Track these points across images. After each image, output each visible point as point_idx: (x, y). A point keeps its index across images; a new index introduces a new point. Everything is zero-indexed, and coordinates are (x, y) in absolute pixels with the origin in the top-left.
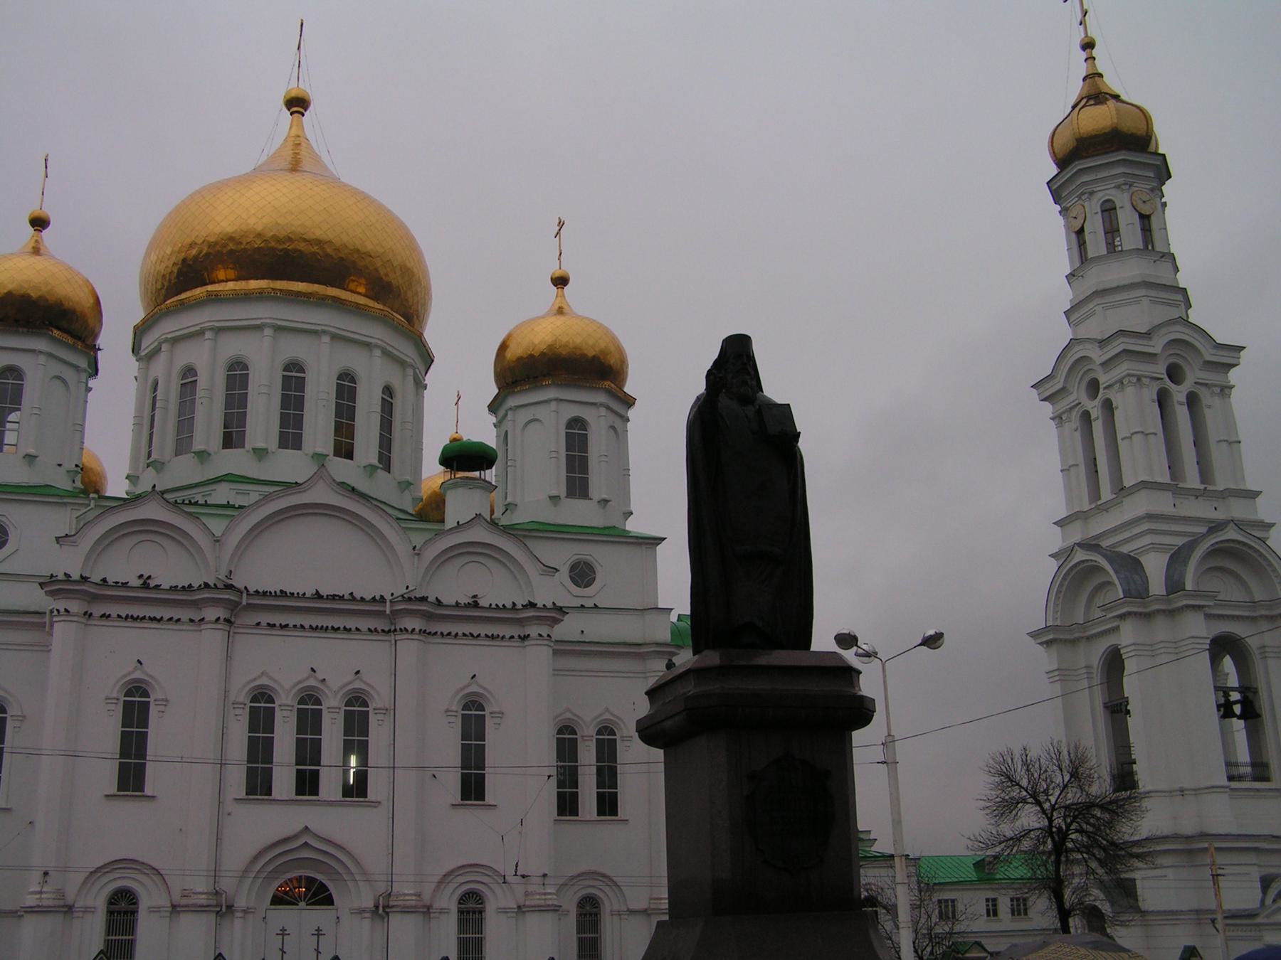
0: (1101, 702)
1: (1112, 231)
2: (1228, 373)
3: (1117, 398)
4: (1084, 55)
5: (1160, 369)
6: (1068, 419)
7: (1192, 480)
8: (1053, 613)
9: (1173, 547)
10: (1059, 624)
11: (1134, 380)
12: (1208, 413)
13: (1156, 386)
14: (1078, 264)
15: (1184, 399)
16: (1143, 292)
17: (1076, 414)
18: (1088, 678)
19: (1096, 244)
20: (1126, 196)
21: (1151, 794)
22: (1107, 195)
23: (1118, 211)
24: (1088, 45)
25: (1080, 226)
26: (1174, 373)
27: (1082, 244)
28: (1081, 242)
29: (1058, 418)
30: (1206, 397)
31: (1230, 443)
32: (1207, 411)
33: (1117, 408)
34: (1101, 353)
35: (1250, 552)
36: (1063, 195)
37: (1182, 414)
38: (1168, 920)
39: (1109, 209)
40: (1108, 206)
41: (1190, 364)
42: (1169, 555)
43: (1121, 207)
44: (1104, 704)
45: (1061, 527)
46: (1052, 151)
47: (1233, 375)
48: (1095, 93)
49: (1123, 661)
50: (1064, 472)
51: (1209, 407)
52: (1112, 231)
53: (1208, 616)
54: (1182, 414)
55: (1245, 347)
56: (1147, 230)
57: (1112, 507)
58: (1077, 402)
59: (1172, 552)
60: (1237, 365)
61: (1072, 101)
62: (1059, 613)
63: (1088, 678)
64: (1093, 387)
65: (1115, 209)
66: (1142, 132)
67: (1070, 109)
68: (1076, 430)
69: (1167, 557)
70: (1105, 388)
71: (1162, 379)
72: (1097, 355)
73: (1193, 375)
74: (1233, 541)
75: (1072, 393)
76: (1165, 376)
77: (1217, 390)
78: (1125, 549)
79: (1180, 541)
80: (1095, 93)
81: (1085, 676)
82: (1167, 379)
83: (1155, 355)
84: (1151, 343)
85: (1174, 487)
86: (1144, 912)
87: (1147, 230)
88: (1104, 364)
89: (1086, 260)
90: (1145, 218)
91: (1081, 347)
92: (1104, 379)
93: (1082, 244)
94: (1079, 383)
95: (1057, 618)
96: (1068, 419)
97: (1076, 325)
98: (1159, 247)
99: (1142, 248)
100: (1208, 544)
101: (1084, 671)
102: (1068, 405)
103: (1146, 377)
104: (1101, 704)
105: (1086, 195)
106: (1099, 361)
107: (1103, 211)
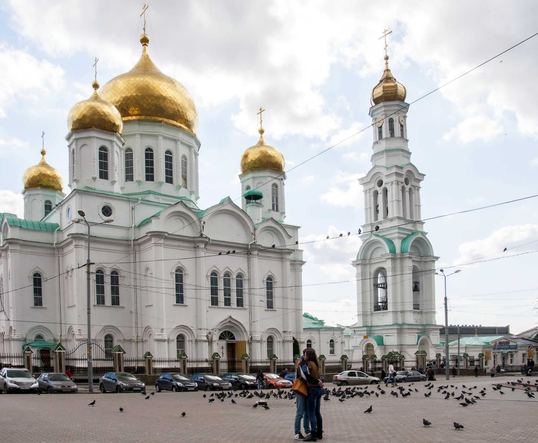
1: (392, 130)
2: (419, 183)
3: (389, 188)
4: (385, 61)
5: (403, 180)
7: (408, 218)
12: (414, 195)
13: (402, 185)
14: (378, 139)
15: (408, 190)
16: (401, 152)
19: (385, 133)
20: (397, 118)
24: (387, 58)
25: (381, 126)
26: (407, 181)
27: (380, 132)
28: (380, 131)
30: (413, 191)
31: (418, 206)
33: (389, 191)
34: (387, 172)
35: (422, 241)
36: (375, 114)
37: (407, 194)
43: (396, 121)
44: (374, 284)
47: (421, 184)
48: (388, 78)
49: (386, 272)
52: (392, 130)
53: (413, 261)
54: (407, 194)
55: (425, 175)
56: (402, 130)
60: (421, 180)
61: (380, 79)
66: (403, 96)
67: (378, 82)
69: (401, 240)
70: (385, 184)
71: (403, 183)
72: (385, 172)
73: (412, 182)
74: (420, 238)
76: (404, 182)
77: (417, 188)
78: (388, 237)
79: (405, 236)
80: (388, 78)
82: (404, 183)
83: (402, 175)
84: (403, 171)
85: (404, 219)
87: (402, 130)
88: (386, 176)
89: (381, 139)
90: (402, 126)
91: (379, 169)
92: (385, 181)
93: (380, 132)
97: (375, 161)
98: (405, 138)
99: (400, 136)
100: (415, 238)
103: (400, 182)
107: (389, 122)
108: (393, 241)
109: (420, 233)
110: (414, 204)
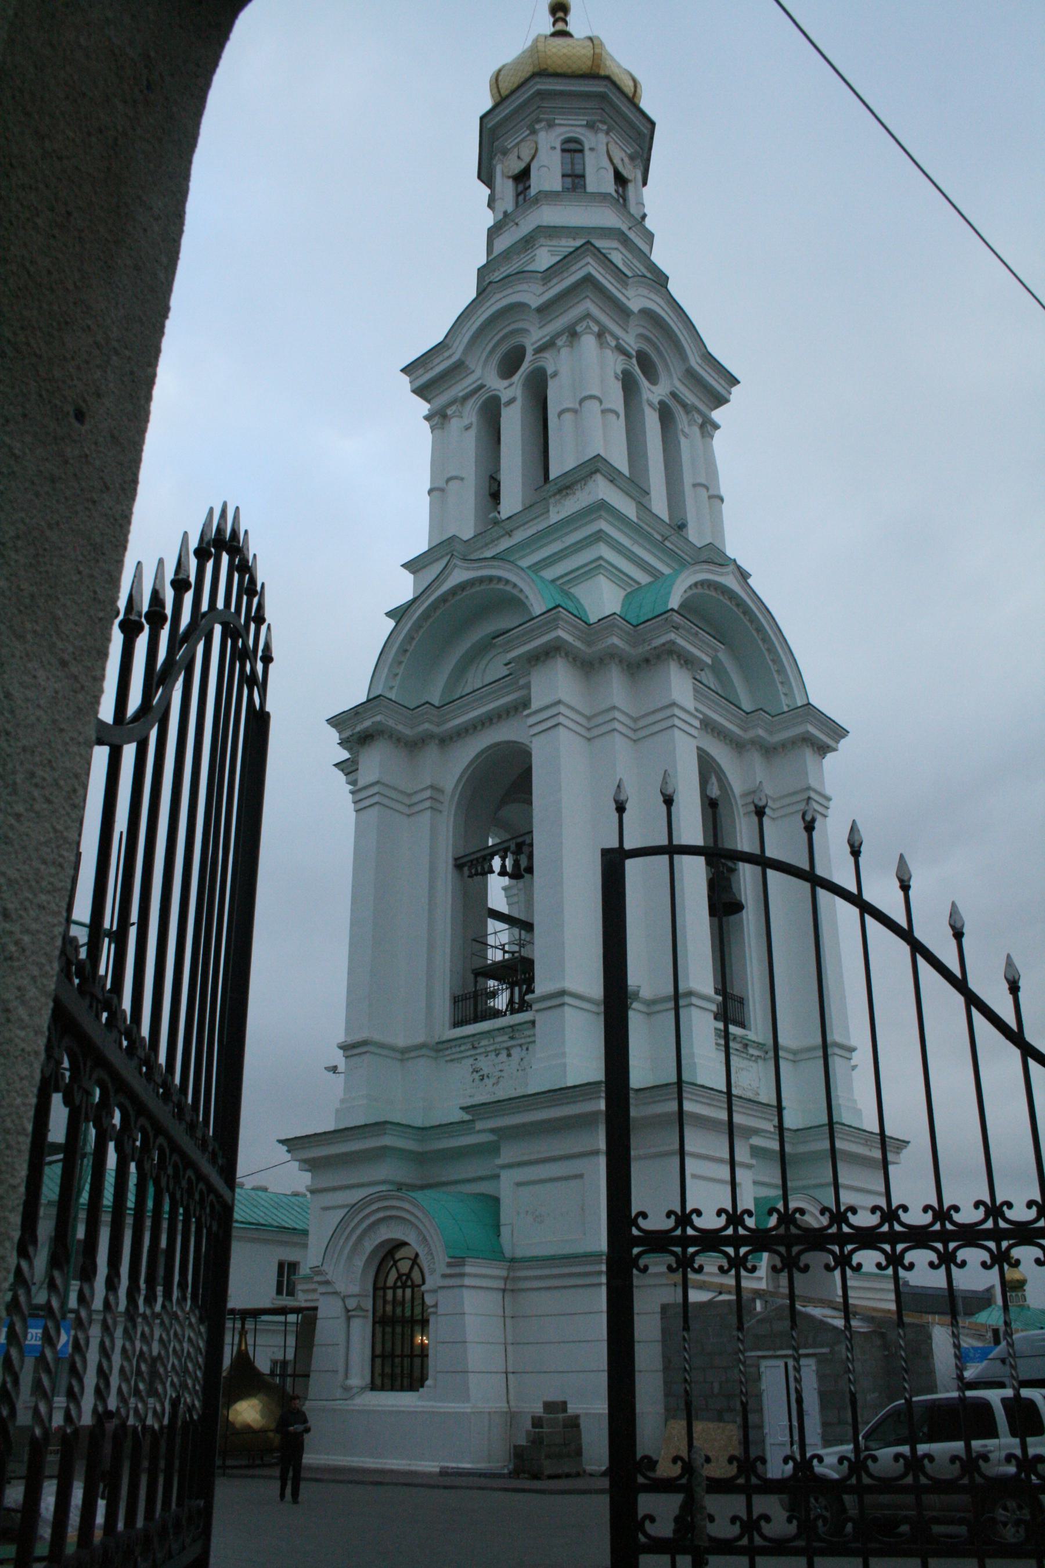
0: (450, 855)
6: (457, 414)
8: (388, 675)
9: (633, 584)
10: (393, 699)
11: (596, 329)
17: (470, 414)
18: (431, 808)
21: (567, 999)
22: (574, 132)
23: (587, 152)
25: (522, 165)
29: (438, 418)
32: (683, 440)
38: (570, 1275)
39: (572, 148)
40: (573, 146)
41: (665, 360)
42: (626, 592)
44: (456, 859)
45: (413, 573)
46: (495, 90)
50: (435, 493)
51: (686, 436)
54: (652, 421)
57: (518, 527)
58: (479, 382)
59: (629, 590)
62: (399, 678)
63: (431, 808)
64: (510, 363)
65: (581, 151)
68: (467, 428)
75: (473, 371)
81: (428, 804)
86: (513, 1261)
88: (541, 310)
94: (488, 357)
95: (396, 675)
96: (457, 414)
101: (428, 793)
102: (463, 390)
104: (451, 862)
105: (543, 124)
106: (535, 302)
107: (563, 151)
108: (572, 590)
109: (732, 567)
110: (688, 480)
